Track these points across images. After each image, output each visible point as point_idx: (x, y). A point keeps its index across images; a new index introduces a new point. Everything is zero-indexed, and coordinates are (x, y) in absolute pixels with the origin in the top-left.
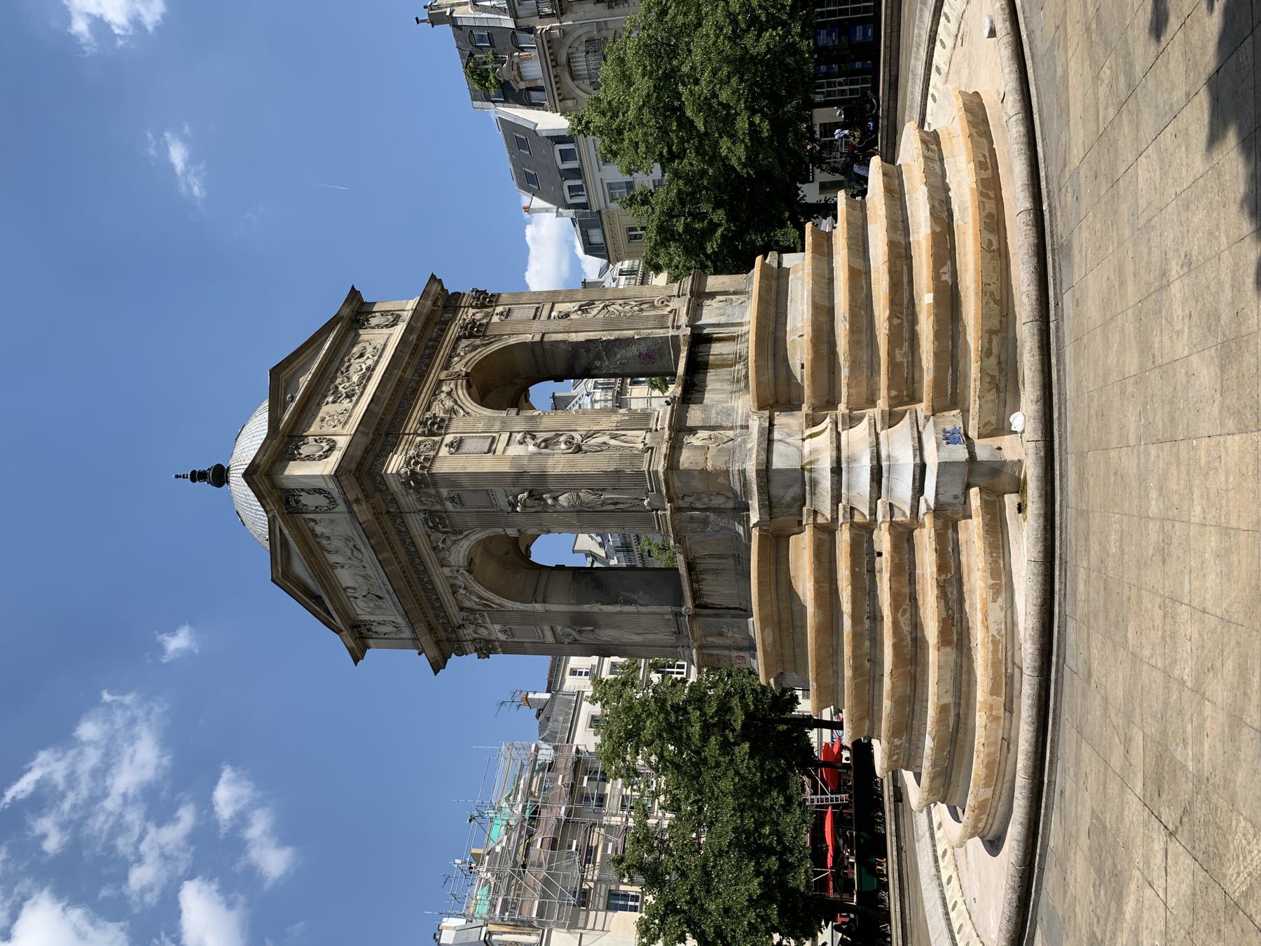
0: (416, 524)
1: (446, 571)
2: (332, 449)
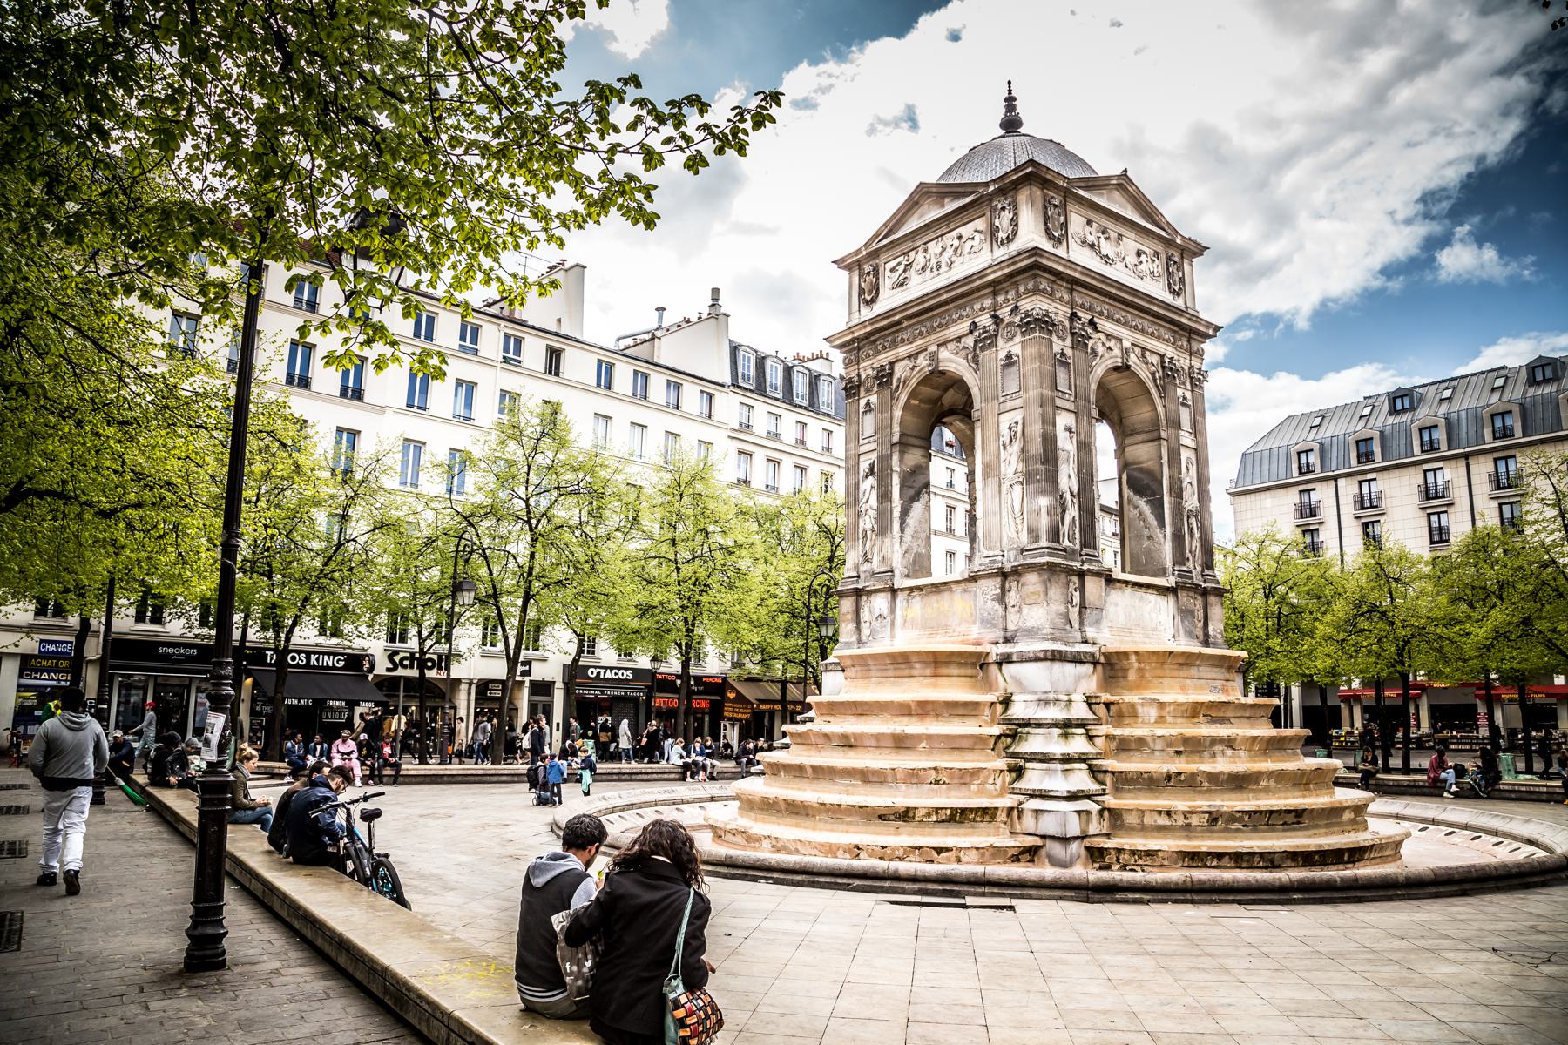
1: (934, 348)
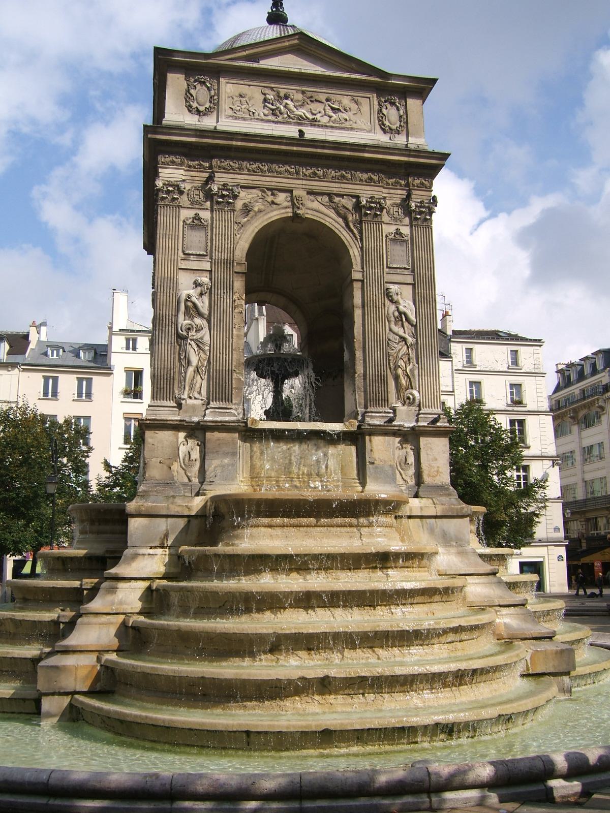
0: (366, 193)
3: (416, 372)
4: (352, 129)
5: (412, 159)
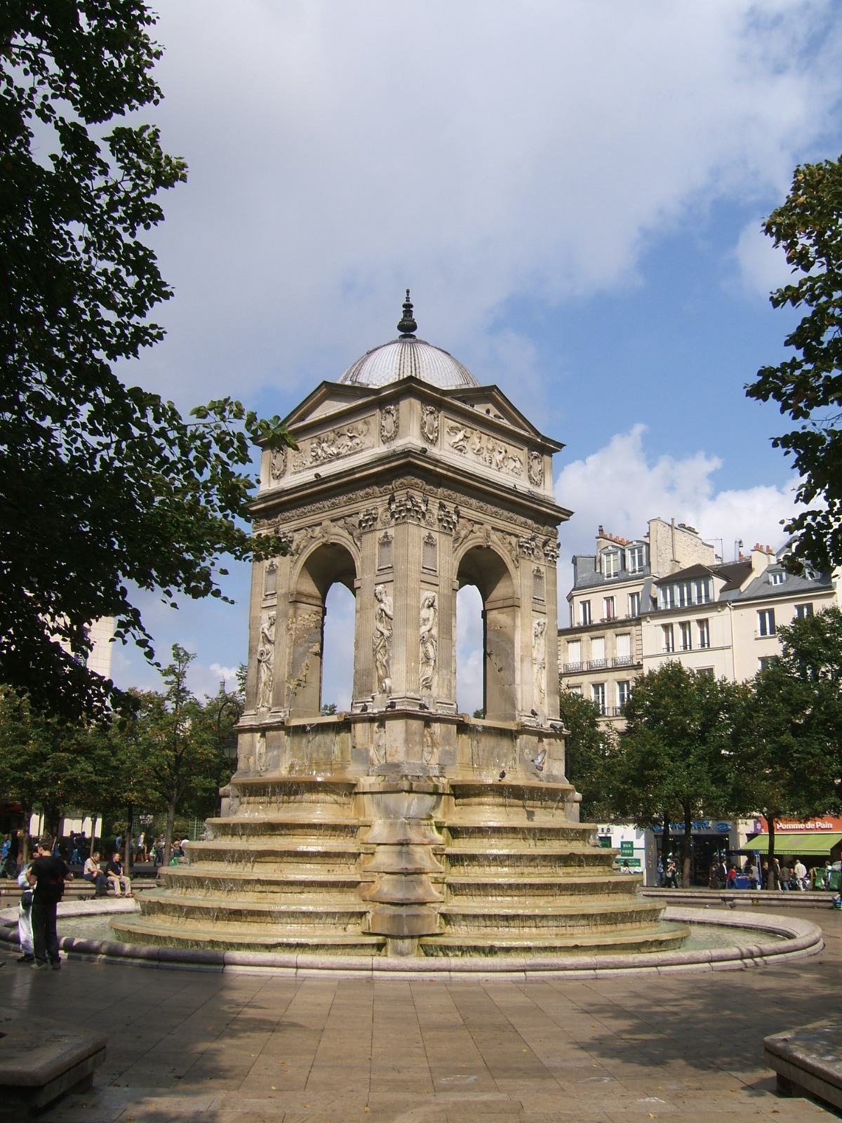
2: (427, 439)
3: (390, 662)
4: (362, 450)
5: (387, 466)
